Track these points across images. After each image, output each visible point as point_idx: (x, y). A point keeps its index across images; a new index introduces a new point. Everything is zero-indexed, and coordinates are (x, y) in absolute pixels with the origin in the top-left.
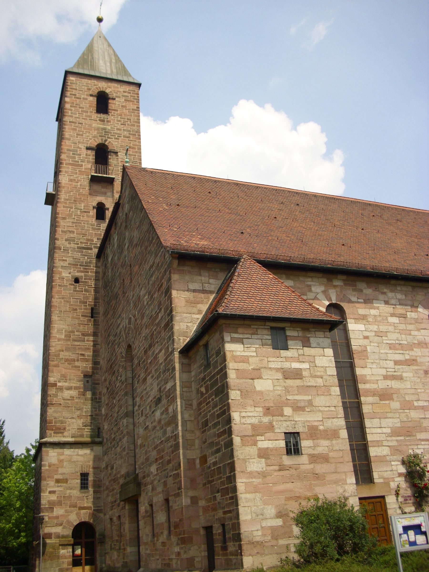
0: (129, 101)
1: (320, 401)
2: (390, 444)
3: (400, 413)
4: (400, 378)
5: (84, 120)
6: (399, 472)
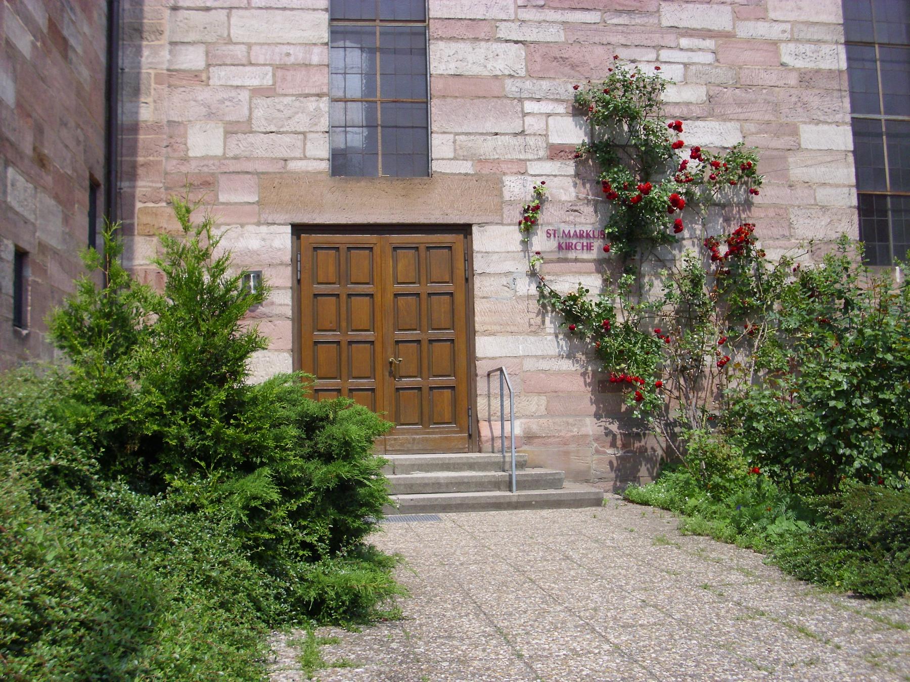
2: (531, 34)
6: (555, 139)
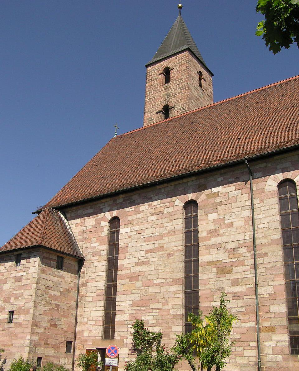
0: (182, 65)
1: (27, 293)
2: (129, 312)
3: (142, 289)
4: (148, 263)
5: (156, 94)
